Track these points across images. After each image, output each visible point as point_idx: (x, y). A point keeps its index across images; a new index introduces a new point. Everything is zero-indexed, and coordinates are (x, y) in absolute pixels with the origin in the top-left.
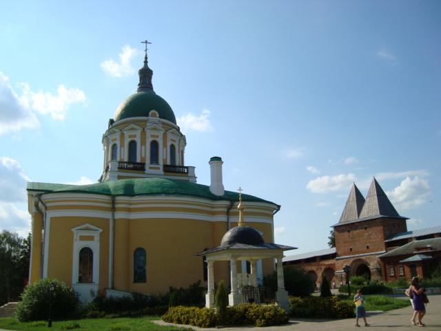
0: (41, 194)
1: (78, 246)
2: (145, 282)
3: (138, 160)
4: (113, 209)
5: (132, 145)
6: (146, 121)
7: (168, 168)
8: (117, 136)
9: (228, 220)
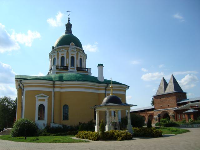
0: (21, 80)
2: (68, 120)
3: (65, 65)
4: (54, 87)
5: (63, 58)
6: (69, 47)
7: (79, 69)
8: (56, 54)
9: (106, 92)
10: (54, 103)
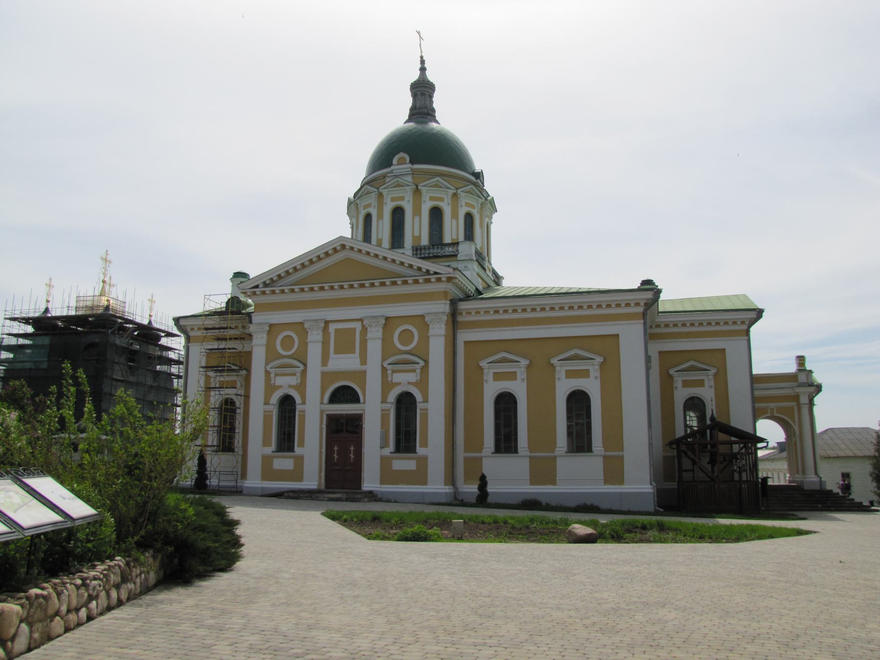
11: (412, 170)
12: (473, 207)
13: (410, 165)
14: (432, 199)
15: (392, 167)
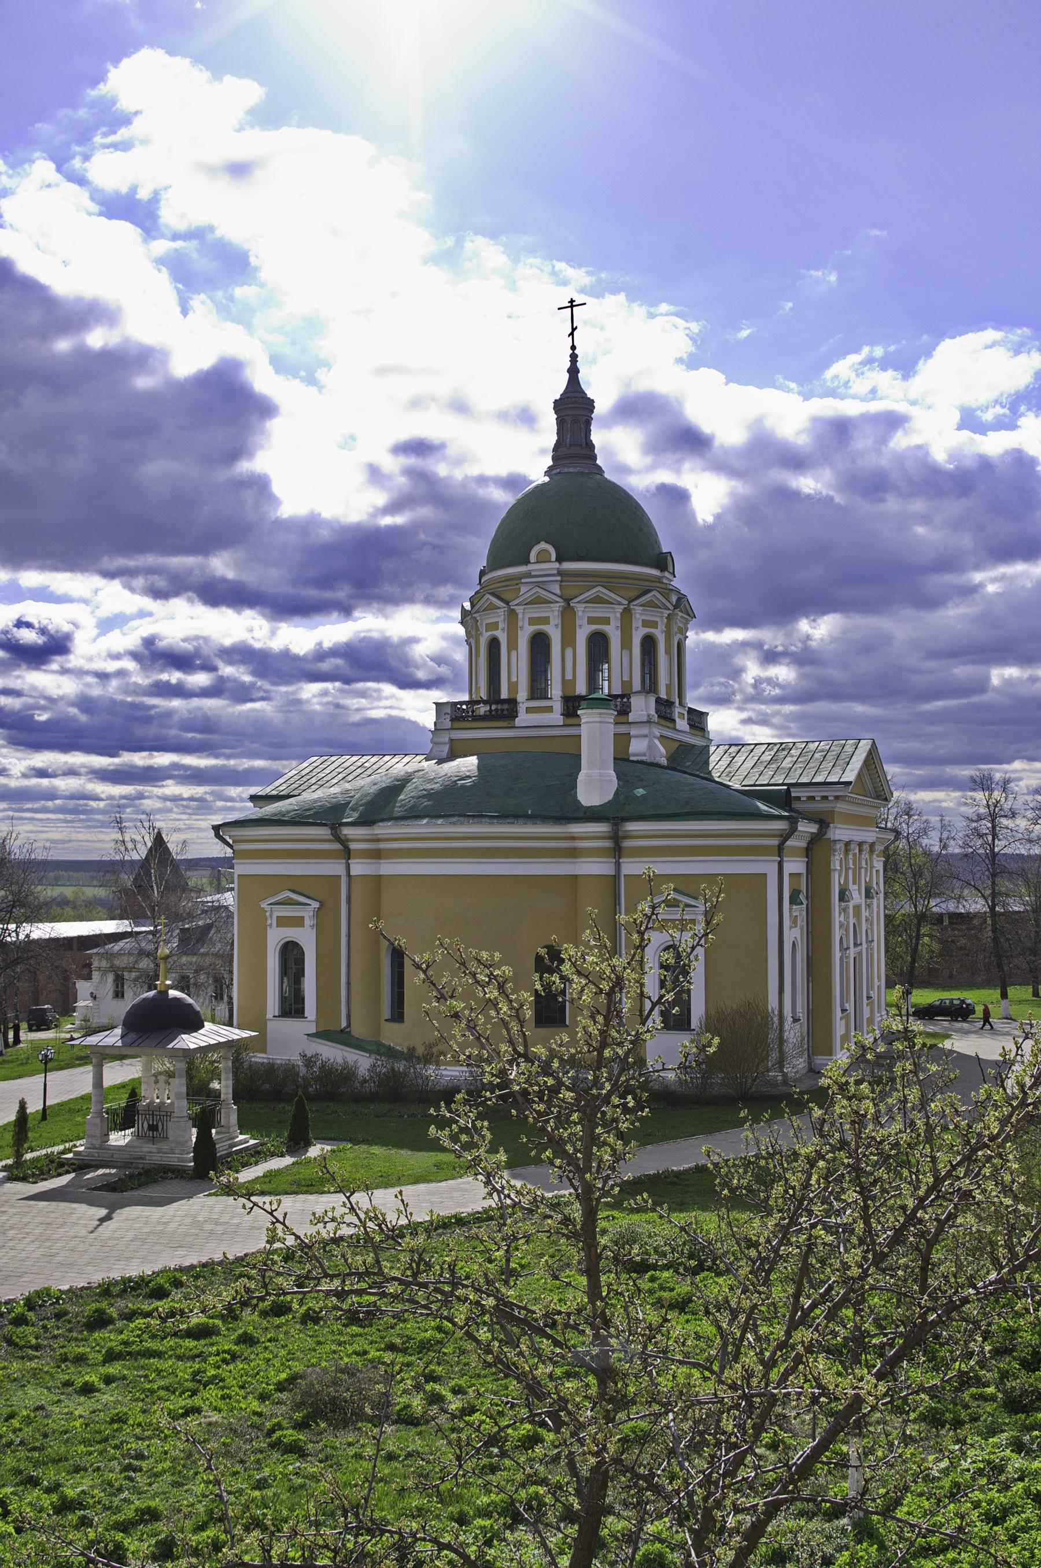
1: (276, 937)
4: (347, 854)
10: (349, 936)
11: (560, 573)
12: (654, 624)
13: (556, 565)
14: (591, 621)
15: (530, 567)
